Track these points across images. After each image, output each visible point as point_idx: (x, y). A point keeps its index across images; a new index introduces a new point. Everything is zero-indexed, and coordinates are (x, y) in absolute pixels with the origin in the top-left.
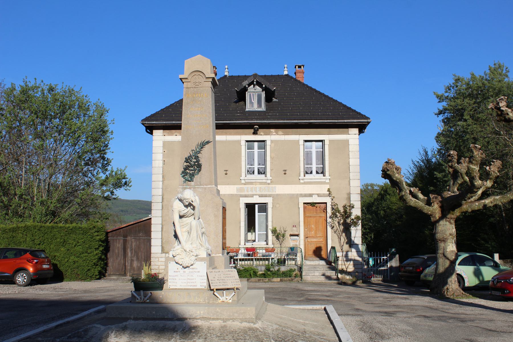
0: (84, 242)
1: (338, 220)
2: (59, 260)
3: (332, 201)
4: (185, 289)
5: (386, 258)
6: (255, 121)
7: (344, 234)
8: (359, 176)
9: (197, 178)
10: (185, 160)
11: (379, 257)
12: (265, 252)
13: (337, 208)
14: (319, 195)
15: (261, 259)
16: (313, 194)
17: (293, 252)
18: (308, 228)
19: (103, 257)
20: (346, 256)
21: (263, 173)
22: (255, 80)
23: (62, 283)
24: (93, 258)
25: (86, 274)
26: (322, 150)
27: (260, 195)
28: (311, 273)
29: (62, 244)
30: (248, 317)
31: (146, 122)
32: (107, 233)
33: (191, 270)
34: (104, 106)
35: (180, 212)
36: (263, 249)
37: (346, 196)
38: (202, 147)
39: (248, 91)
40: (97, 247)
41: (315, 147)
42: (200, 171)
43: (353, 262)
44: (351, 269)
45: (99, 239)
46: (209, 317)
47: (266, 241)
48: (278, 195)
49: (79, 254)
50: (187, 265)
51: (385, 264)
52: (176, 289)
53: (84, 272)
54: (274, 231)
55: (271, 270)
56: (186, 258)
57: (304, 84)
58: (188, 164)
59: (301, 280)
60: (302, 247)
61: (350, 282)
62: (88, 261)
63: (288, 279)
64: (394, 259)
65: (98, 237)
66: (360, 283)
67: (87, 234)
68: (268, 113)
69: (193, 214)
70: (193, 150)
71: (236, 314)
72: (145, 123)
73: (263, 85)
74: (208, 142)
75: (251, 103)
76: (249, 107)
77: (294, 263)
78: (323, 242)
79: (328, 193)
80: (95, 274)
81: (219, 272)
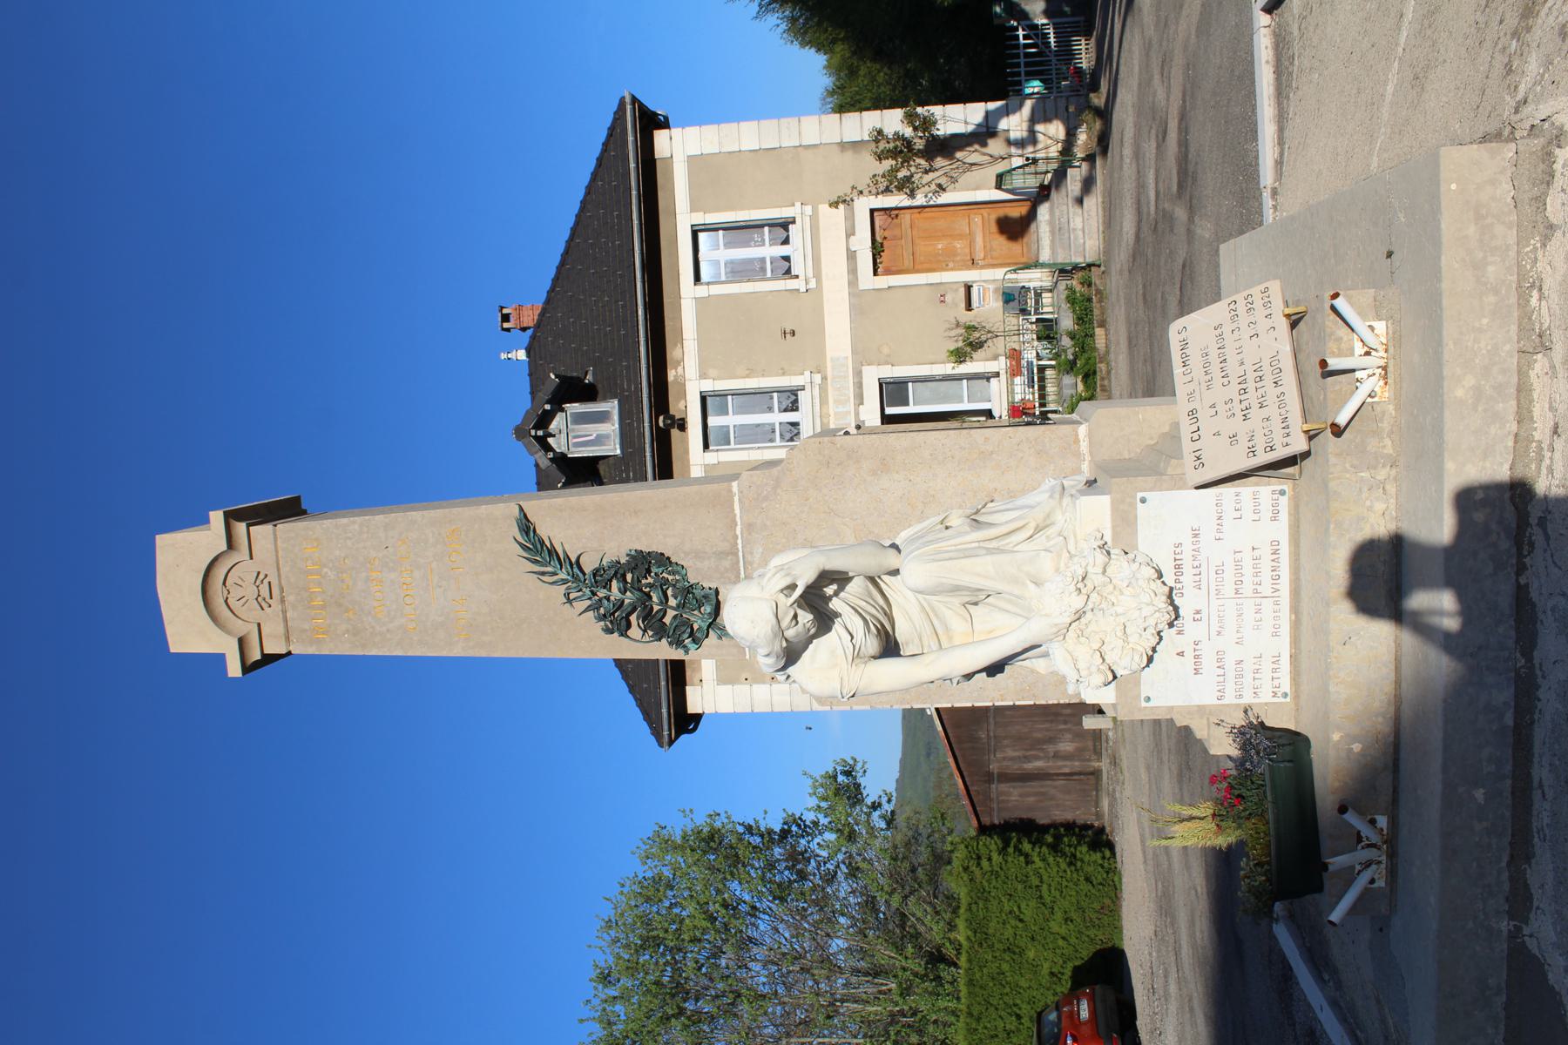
0: (1011, 895)
1: (920, 174)
2: (1061, 962)
3: (866, 192)
4: (1295, 609)
5: (1023, 30)
6: (647, 424)
7: (959, 155)
8: (789, 120)
9: (700, 574)
10: (616, 634)
11: (1021, 51)
12: (1019, 377)
13: (884, 176)
14: (850, 232)
15: (1042, 388)
16: (848, 249)
17: (1017, 296)
18: (945, 261)
19: (1049, 839)
20: (1020, 144)
21: (793, 398)
22: (533, 432)
23: (1126, 951)
24: (1055, 869)
25: (1101, 887)
26: (721, 232)
27: (857, 402)
28: (1076, 239)
29: (1015, 957)
30: (1505, 190)
31: (666, 733)
32: (983, 830)
33: (1188, 579)
34: (649, 838)
35: (857, 656)
36: (1012, 384)
37: (849, 155)
38: (549, 552)
39: (566, 451)
40: (1022, 859)
41: (714, 251)
42: (663, 560)
43: (1038, 123)
44: (1057, 129)
45: (999, 854)
46: (1511, 444)
47: (988, 379)
48: (854, 352)
49: (1043, 908)
50: (1161, 602)
51: (1040, 32)
52: (1295, 659)
53: (1093, 891)
54: (960, 356)
55: (1071, 357)
56: (1119, 610)
57: (548, 301)
58: (633, 618)
59: (1099, 266)
60: (999, 273)
61: (1098, 125)
62: (1065, 883)
63: (1098, 305)
64: (1023, 6)
65: (995, 856)
66: (1099, 98)
67: (987, 888)
68: (623, 390)
69: (872, 580)
70: (567, 595)
71: (1491, 269)
72: (666, 737)
73: (545, 411)
74: (526, 526)
75: (599, 440)
76: (612, 447)
77: (1050, 295)
78: (985, 215)
79: (841, 206)
80: (1100, 862)
81: (1192, 413)
